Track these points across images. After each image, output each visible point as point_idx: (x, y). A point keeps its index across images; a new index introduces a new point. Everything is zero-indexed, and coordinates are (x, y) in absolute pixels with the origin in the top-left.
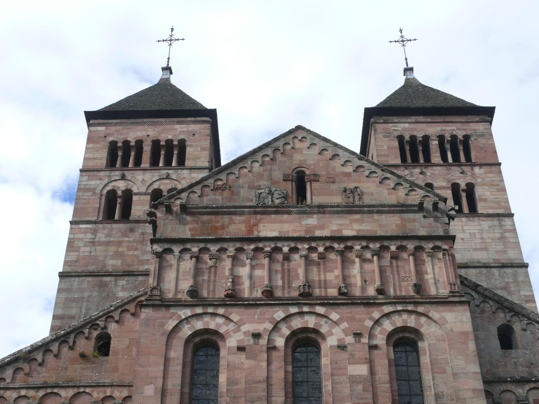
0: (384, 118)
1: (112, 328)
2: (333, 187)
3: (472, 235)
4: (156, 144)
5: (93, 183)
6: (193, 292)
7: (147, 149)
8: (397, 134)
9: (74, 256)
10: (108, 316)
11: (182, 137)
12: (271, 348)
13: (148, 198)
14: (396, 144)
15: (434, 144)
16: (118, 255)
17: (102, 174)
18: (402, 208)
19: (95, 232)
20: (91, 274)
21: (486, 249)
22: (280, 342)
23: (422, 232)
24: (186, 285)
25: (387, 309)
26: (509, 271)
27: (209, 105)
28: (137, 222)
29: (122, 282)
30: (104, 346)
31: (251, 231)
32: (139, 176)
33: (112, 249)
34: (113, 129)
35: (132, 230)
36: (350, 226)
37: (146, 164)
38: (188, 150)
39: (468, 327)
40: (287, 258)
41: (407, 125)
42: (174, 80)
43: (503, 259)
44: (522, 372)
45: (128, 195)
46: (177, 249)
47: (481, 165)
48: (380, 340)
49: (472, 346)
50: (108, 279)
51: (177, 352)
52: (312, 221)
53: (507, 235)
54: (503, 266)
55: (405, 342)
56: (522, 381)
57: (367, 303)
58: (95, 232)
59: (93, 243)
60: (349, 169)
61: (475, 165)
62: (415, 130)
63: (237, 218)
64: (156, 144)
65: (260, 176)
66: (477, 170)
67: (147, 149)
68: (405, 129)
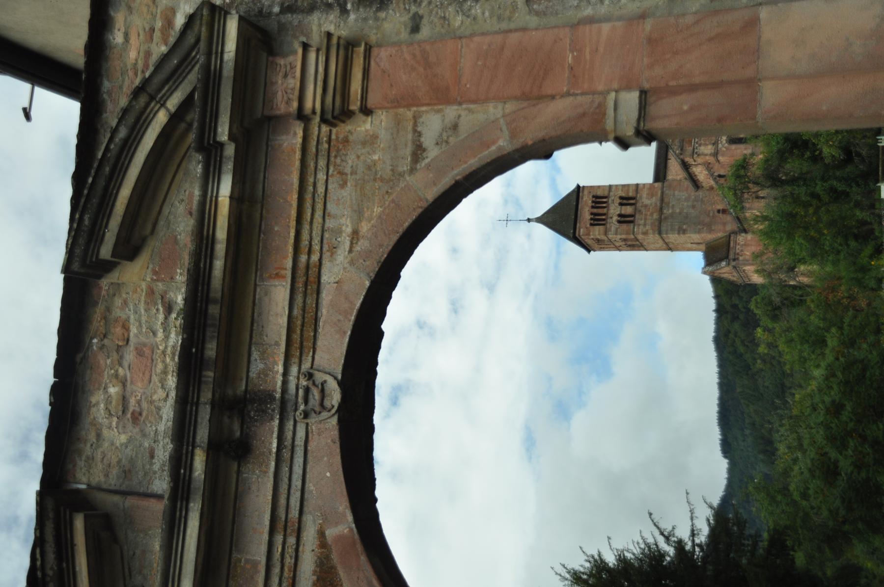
1: (716, 174)
4: (593, 207)
5: (613, 229)
6: (714, 144)
7: (595, 211)
9: (650, 231)
10: (712, 175)
13: (623, 207)
16: (652, 214)
19: (639, 225)
20: (660, 223)
24: (710, 147)
27: (573, 187)
28: (636, 209)
29: (665, 211)
30: (720, 176)
32: (612, 211)
37: (605, 211)
38: (599, 193)
42: (539, 214)
45: (620, 215)
51: (733, 147)
58: (639, 225)
59: (645, 225)
64: (593, 207)
67: (595, 211)
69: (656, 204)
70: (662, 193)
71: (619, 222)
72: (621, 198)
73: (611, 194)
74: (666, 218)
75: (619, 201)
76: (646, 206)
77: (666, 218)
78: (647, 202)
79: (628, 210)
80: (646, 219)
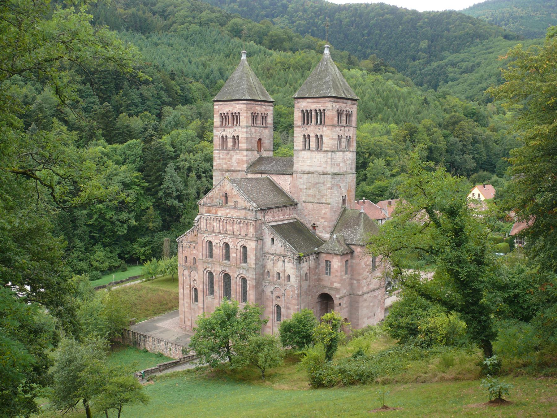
0: (299, 100)
2: (232, 199)
3: (318, 159)
4: (232, 113)
7: (230, 116)
8: (301, 109)
11: (239, 111)
12: (220, 247)
14: (300, 114)
15: (313, 113)
16: (226, 163)
17: (219, 129)
18: (245, 209)
19: (219, 154)
21: (321, 166)
22: (222, 245)
23: (249, 218)
25: (240, 240)
26: (326, 176)
31: (216, 213)
33: (224, 161)
34: (221, 107)
35: (228, 154)
36: (235, 214)
39: (254, 247)
40: (223, 222)
41: (305, 104)
43: (325, 171)
44: (273, 252)
46: (203, 216)
47: (326, 126)
48: (239, 248)
49: (255, 252)
50: (224, 172)
51: (204, 245)
52: (228, 211)
53: (329, 160)
54: (324, 174)
55: (245, 248)
56: (273, 255)
57: (237, 237)
58: (219, 154)
60: (236, 194)
61: (323, 126)
62: (307, 107)
63: (214, 208)
65: (217, 194)
66: (325, 128)
67: (230, 116)
68: (304, 107)
69: (232, 166)
70: (239, 171)
71: (222, 136)
72: (238, 136)
73: (240, 128)
74: (223, 175)
75: (235, 135)
76: (231, 158)
77: (223, 175)
78: (234, 159)
79: (230, 144)
80: (223, 159)
